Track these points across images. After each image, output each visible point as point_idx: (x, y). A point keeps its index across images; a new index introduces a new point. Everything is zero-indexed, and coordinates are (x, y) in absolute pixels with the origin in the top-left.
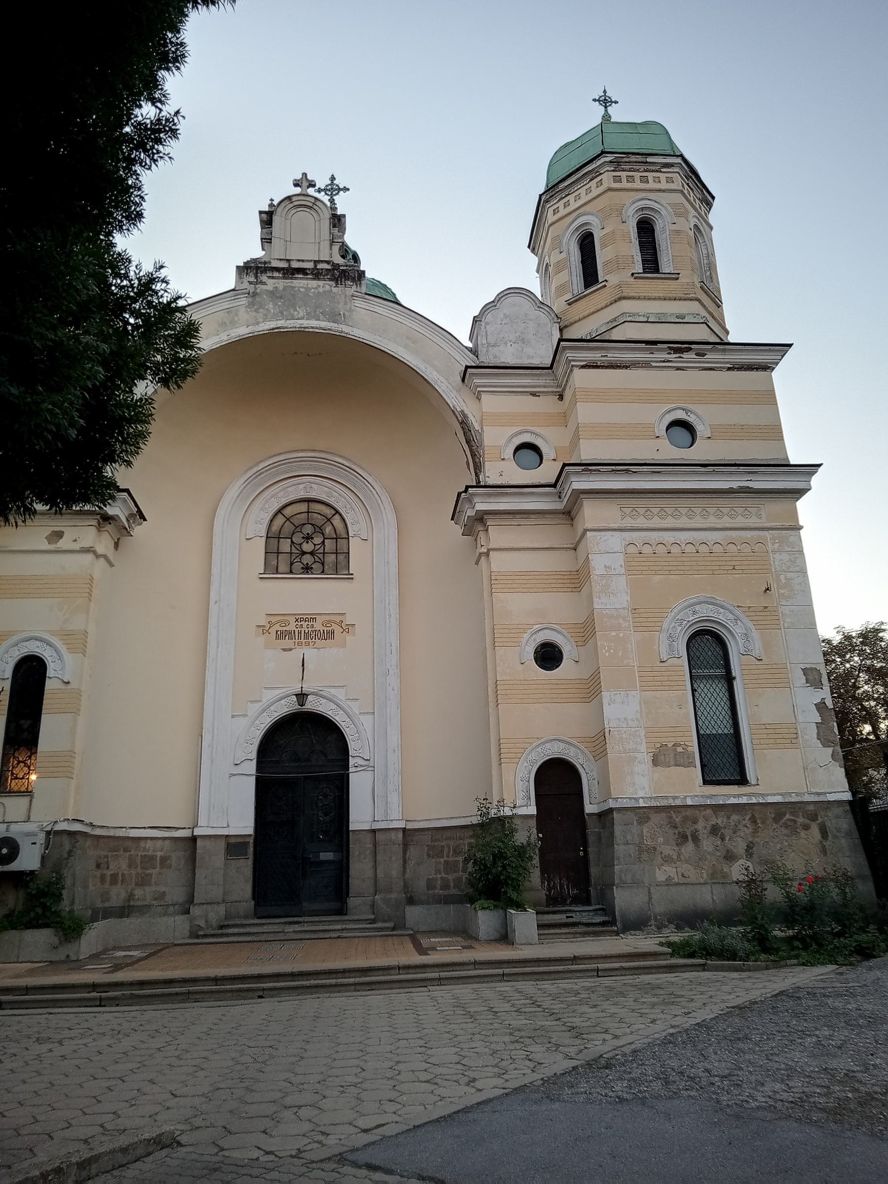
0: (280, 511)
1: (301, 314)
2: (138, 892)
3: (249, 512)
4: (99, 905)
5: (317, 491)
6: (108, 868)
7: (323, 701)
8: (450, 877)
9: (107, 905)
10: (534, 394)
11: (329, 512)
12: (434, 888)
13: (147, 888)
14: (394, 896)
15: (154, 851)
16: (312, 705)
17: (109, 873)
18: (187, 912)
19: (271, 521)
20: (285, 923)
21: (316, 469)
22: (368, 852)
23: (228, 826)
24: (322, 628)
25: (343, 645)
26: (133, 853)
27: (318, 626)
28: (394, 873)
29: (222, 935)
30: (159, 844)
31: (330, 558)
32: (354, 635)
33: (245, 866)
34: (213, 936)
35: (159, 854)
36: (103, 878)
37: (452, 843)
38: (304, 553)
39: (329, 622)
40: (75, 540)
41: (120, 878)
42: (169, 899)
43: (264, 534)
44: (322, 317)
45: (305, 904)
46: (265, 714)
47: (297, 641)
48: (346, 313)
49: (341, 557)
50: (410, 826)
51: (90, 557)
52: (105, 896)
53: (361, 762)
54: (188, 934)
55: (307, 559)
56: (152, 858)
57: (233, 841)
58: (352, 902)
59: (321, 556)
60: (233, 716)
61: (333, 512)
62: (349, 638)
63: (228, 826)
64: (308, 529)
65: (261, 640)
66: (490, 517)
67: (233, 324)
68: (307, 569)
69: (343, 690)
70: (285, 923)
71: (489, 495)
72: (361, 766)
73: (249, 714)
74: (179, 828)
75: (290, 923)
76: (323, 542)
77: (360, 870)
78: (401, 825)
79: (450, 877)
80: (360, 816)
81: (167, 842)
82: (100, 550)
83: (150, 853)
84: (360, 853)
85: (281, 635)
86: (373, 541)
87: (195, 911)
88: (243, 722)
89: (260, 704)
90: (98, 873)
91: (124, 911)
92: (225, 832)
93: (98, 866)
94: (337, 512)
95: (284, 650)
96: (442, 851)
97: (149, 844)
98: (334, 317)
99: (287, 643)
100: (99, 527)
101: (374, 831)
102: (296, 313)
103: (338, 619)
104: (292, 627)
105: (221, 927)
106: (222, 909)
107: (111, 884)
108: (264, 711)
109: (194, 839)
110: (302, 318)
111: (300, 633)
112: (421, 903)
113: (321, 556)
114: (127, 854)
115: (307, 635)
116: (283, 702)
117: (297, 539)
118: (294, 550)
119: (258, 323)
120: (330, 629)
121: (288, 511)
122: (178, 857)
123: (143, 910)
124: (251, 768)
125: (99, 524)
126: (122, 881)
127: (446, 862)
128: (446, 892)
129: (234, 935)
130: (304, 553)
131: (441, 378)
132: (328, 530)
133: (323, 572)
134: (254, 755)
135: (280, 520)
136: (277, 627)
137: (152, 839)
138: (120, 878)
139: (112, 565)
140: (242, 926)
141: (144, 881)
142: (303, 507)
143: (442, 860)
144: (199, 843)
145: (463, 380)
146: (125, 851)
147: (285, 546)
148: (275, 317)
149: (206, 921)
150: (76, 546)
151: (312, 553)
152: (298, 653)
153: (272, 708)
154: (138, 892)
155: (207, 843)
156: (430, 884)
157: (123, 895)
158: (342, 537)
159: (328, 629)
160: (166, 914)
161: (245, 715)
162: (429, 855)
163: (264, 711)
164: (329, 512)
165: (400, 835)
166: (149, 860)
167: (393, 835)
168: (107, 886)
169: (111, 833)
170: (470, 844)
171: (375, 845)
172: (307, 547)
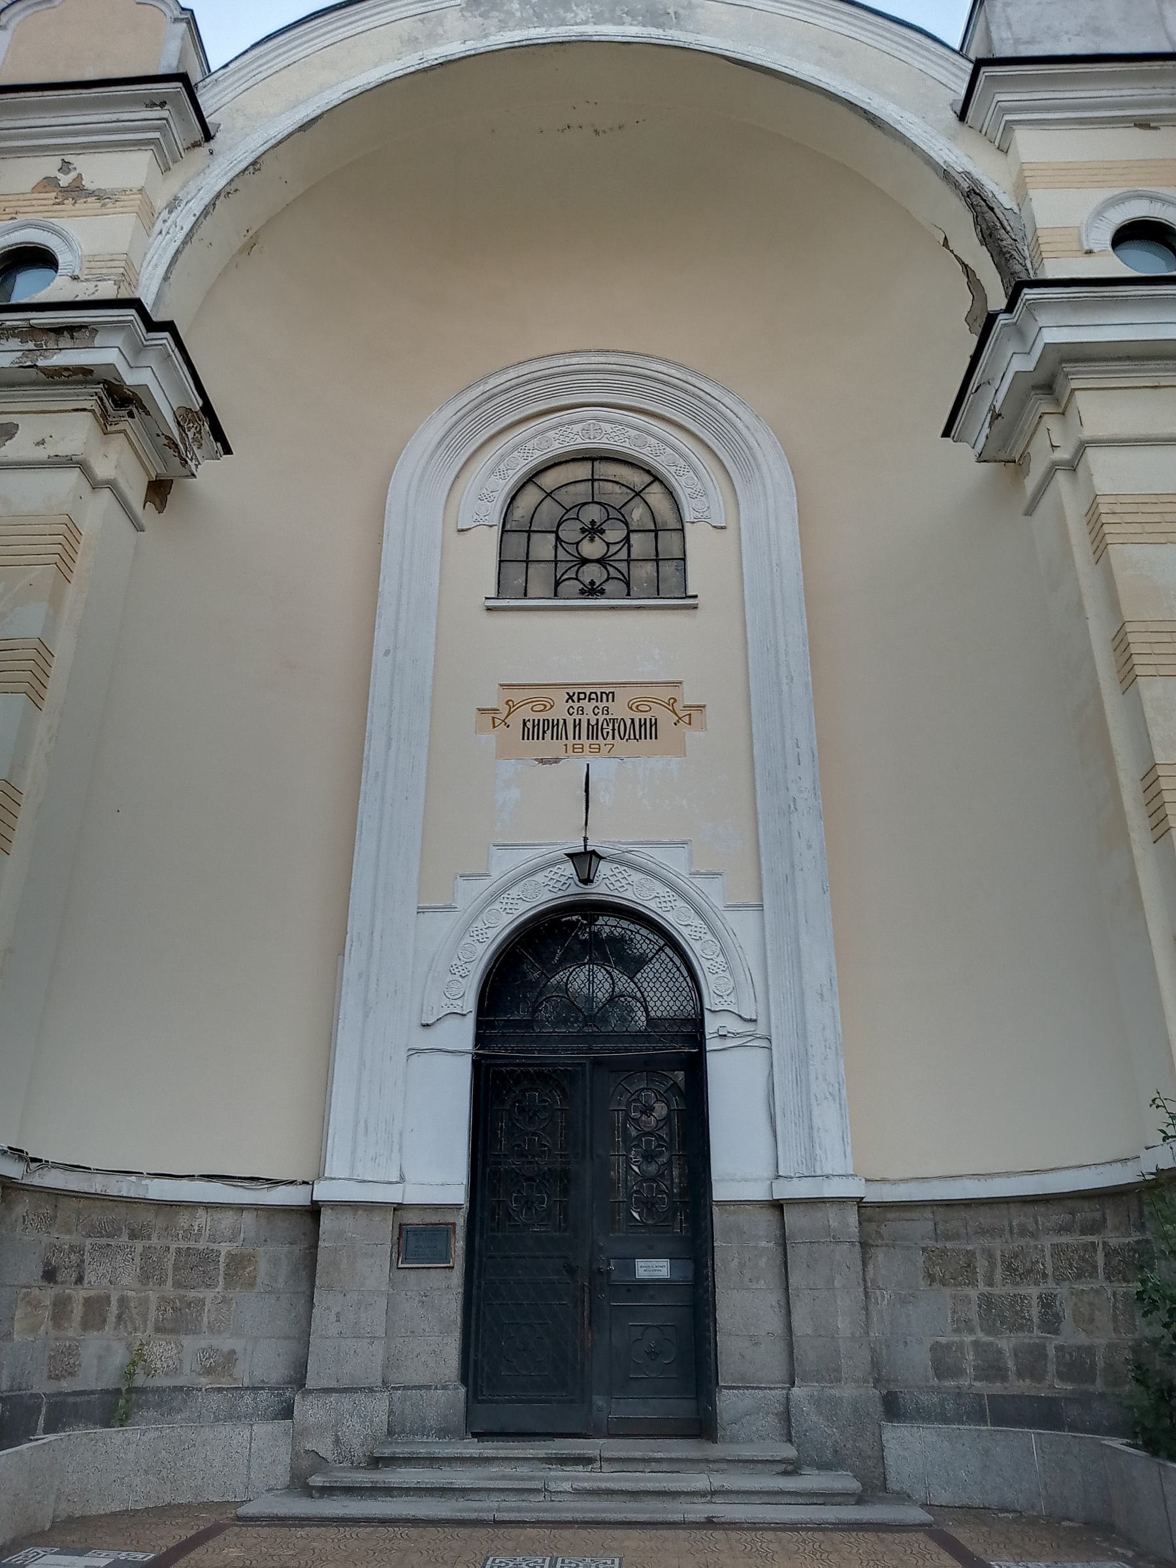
0: (532, 478)
1: (582, 16)
2: (161, 1351)
3: (462, 481)
4: (41, 1386)
5: (611, 434)
6: (80, 1280)
7: (636, 877)
8: (1006, 1343)
9: (66, 1385)
10: (1143, 124)
11: (637, 479)
12: (957, 1372)
13: (187, 1340)
14: (846, 1392)
15: (213, 1239)
16: (609, 883)
17: (80, 1294)
18: (287, 1412)
19: (513, 498)
20: (548, 1460)
21: (610, 390)
22: (763, 1262)
23: (402, 1179)
24: (628, 716)
25: (680, 750)
26: (154, 1241)
27: (619, 710)
28: (843, 1325)
29: (374, 1491)
30: (227, 1220)
31: (643, 572)
32: (703, 728)
33: (444, 1288)
34: (351, 1491)
35: (225, 1248)
36: (61, 1308)
37: (998, 1246)
38: (584, 561)
39: (646, 700)
40: (43, 442)
41: (114, 1308)
42: (243, 1374)
43: (496, 518)
44: (628, 19)
45: (599, 1401)
46: (497, 906)
47: (571, 741)
48: (681, 11)
49: (667, 569)
50: (874, 1194)
51: (73, 476)
52: (63, 1363)
53: (732, 1025)
54: (285, 1479)
55: (592, 573)
56: (208, 1258)
57: (412, 1218)
58: (728, 1402)
59: (623, 566)
60: (421, 911)
61: (647, 479)
62: (692, 736)
63: (402, 1179)
64: (593, 513)
65: (489, 739)
66: (1081, 367)
67: (433, 39)
68: (592, 590)
69: (683, 853)
70: (548, 1460)
71: (1075, 305)
72: (736, 1035)
73: (460, 905)
74: (277, 1183)
75: (563, 1461)
76: (627, 539)
77: (744, 1311)
78: (853, 1189)
79: (1006, 1343)
80: (741, 1164)
81: (248, 1218)
82: (103, 469)
83: (202, 1245)
84: (742, 1265)
85: (534, 730)
86: (743, 526)
87: (308, 1410)
88: (442, 926)
89: (486, 882)
90: (48, 1295)
91: (114, 1407)
92: (392, 1195)
93: (50, 1275)
94: (656, 478)
95: (541, 761)
96: (970, 1266)
97: (202, 1217)
98: (655, 17)
99: (549, 746)
100: (105, 421)
101: (778, 1206)
102: (570, 15)
103: (665, 694)
104: (560, 711)
105: (376, 1462)
106: (378, 1408)
107: (86, 1325)
108: (495, 897)
109: (314, 1211)
110: (585, 23)
111: (577, 725)
112: (923, 1415)
113: (623, 566)
114: (139, 1245)
115: (594, 731)
116: (539, 878)
117: (570, 532)
118: (562, 555)
119: (486, 36)
120: (648, 716)
121: (549, 480)
122: (273, 1260)
123: (171, 1400)
124: (462, 1034)
125: (105, 414)
126: (119, 1317)
127: (987, 1302)
128: (997, 1388)
129: (406, 1491)
130: (584, 561)
131: (906, 115)
132: (637, 514)
133: (628, 594)
134: (470, 1004)
135: (531, 497)
136: (526, 713)
137: (209, 1206)
138: (114, 1308)
139: (139, 528)
140: (432, 1461)
141: (179, 1320)
142: (582, 471)
143: (973, 1293)
144: (327, 1220)
145: (962, 116)
146: (133, 1236)
147: (544, 547)
148: (524, 23)
149: (337, 1441)
150: (41, 454)
151: (602, 561)
152: (573, 768)
153: (514, 892)
154: (161, 1351)
155: (348, 1222)
156: (944, 1363)
157: (119, 1358)
158: (668, 530)
159: (643, 716)
160: (233, 1416)
161: (449, 908)
162: (931, 1278)
163: (495, 897)
164: (637, 479)
165: (852, 1218)
166: (197, 1264)
167: (833, 1217)
168: (72, 1330)
169: (96, 1185)
170: (1058, 1250)
171: (783, 1242)
172: (593, 549)
